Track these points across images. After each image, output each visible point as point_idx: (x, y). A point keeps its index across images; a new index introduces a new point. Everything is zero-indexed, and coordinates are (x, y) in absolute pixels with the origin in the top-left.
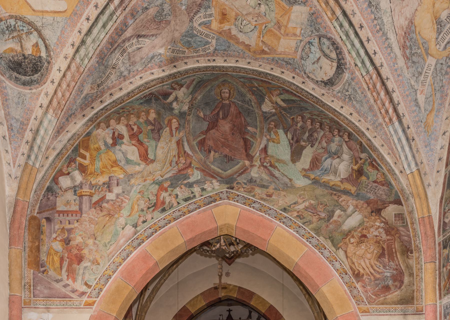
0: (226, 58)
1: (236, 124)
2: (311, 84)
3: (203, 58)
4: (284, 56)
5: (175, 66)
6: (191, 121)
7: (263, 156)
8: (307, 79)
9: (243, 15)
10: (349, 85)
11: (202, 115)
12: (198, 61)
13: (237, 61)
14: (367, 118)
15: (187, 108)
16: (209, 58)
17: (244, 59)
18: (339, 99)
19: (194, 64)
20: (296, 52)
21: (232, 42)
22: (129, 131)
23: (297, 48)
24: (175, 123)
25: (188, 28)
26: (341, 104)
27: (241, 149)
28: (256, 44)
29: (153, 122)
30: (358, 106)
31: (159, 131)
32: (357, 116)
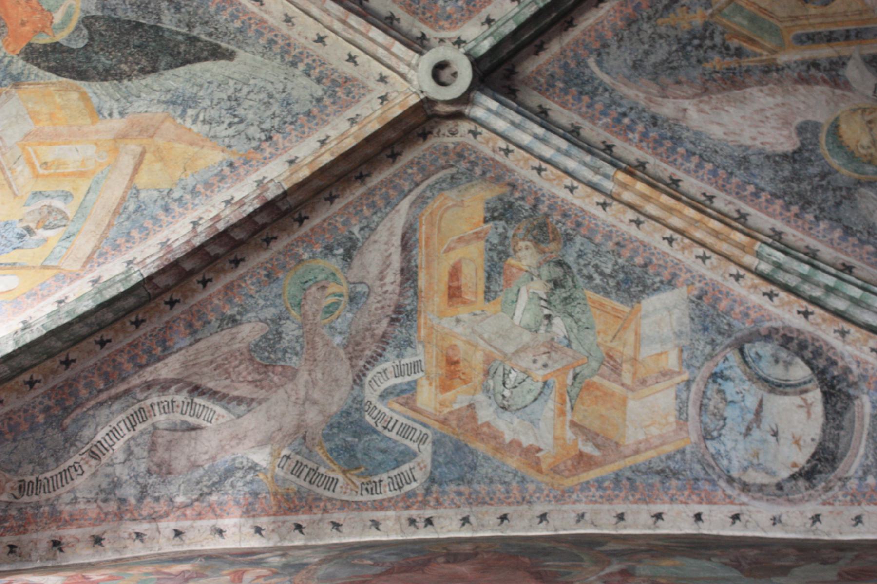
0: (465, 511)
3: (391, 513)
4: (651, 454)
5: (299, 527)
8: (744, 498)
9: (505, 355)
12: (376, 524)
13: (504, 518)
16: (414, 513)
17: (525, 507)
19: (361, 534)
21: (481, 447)
25: (349, 402)
28: (556, 438)
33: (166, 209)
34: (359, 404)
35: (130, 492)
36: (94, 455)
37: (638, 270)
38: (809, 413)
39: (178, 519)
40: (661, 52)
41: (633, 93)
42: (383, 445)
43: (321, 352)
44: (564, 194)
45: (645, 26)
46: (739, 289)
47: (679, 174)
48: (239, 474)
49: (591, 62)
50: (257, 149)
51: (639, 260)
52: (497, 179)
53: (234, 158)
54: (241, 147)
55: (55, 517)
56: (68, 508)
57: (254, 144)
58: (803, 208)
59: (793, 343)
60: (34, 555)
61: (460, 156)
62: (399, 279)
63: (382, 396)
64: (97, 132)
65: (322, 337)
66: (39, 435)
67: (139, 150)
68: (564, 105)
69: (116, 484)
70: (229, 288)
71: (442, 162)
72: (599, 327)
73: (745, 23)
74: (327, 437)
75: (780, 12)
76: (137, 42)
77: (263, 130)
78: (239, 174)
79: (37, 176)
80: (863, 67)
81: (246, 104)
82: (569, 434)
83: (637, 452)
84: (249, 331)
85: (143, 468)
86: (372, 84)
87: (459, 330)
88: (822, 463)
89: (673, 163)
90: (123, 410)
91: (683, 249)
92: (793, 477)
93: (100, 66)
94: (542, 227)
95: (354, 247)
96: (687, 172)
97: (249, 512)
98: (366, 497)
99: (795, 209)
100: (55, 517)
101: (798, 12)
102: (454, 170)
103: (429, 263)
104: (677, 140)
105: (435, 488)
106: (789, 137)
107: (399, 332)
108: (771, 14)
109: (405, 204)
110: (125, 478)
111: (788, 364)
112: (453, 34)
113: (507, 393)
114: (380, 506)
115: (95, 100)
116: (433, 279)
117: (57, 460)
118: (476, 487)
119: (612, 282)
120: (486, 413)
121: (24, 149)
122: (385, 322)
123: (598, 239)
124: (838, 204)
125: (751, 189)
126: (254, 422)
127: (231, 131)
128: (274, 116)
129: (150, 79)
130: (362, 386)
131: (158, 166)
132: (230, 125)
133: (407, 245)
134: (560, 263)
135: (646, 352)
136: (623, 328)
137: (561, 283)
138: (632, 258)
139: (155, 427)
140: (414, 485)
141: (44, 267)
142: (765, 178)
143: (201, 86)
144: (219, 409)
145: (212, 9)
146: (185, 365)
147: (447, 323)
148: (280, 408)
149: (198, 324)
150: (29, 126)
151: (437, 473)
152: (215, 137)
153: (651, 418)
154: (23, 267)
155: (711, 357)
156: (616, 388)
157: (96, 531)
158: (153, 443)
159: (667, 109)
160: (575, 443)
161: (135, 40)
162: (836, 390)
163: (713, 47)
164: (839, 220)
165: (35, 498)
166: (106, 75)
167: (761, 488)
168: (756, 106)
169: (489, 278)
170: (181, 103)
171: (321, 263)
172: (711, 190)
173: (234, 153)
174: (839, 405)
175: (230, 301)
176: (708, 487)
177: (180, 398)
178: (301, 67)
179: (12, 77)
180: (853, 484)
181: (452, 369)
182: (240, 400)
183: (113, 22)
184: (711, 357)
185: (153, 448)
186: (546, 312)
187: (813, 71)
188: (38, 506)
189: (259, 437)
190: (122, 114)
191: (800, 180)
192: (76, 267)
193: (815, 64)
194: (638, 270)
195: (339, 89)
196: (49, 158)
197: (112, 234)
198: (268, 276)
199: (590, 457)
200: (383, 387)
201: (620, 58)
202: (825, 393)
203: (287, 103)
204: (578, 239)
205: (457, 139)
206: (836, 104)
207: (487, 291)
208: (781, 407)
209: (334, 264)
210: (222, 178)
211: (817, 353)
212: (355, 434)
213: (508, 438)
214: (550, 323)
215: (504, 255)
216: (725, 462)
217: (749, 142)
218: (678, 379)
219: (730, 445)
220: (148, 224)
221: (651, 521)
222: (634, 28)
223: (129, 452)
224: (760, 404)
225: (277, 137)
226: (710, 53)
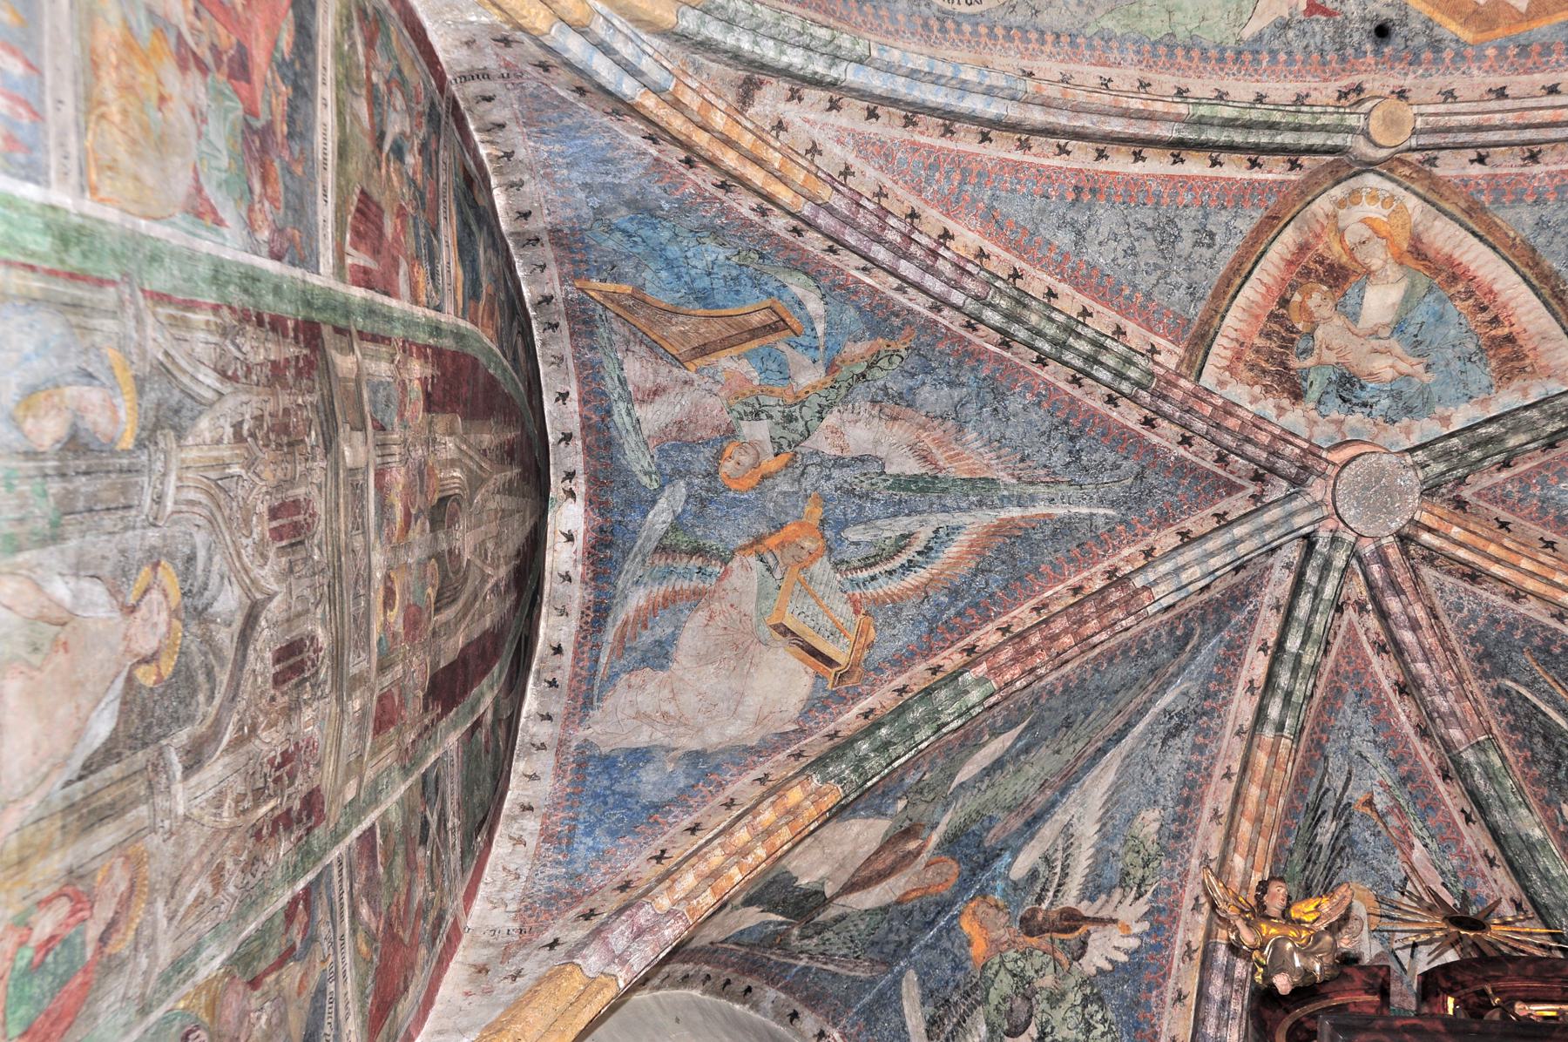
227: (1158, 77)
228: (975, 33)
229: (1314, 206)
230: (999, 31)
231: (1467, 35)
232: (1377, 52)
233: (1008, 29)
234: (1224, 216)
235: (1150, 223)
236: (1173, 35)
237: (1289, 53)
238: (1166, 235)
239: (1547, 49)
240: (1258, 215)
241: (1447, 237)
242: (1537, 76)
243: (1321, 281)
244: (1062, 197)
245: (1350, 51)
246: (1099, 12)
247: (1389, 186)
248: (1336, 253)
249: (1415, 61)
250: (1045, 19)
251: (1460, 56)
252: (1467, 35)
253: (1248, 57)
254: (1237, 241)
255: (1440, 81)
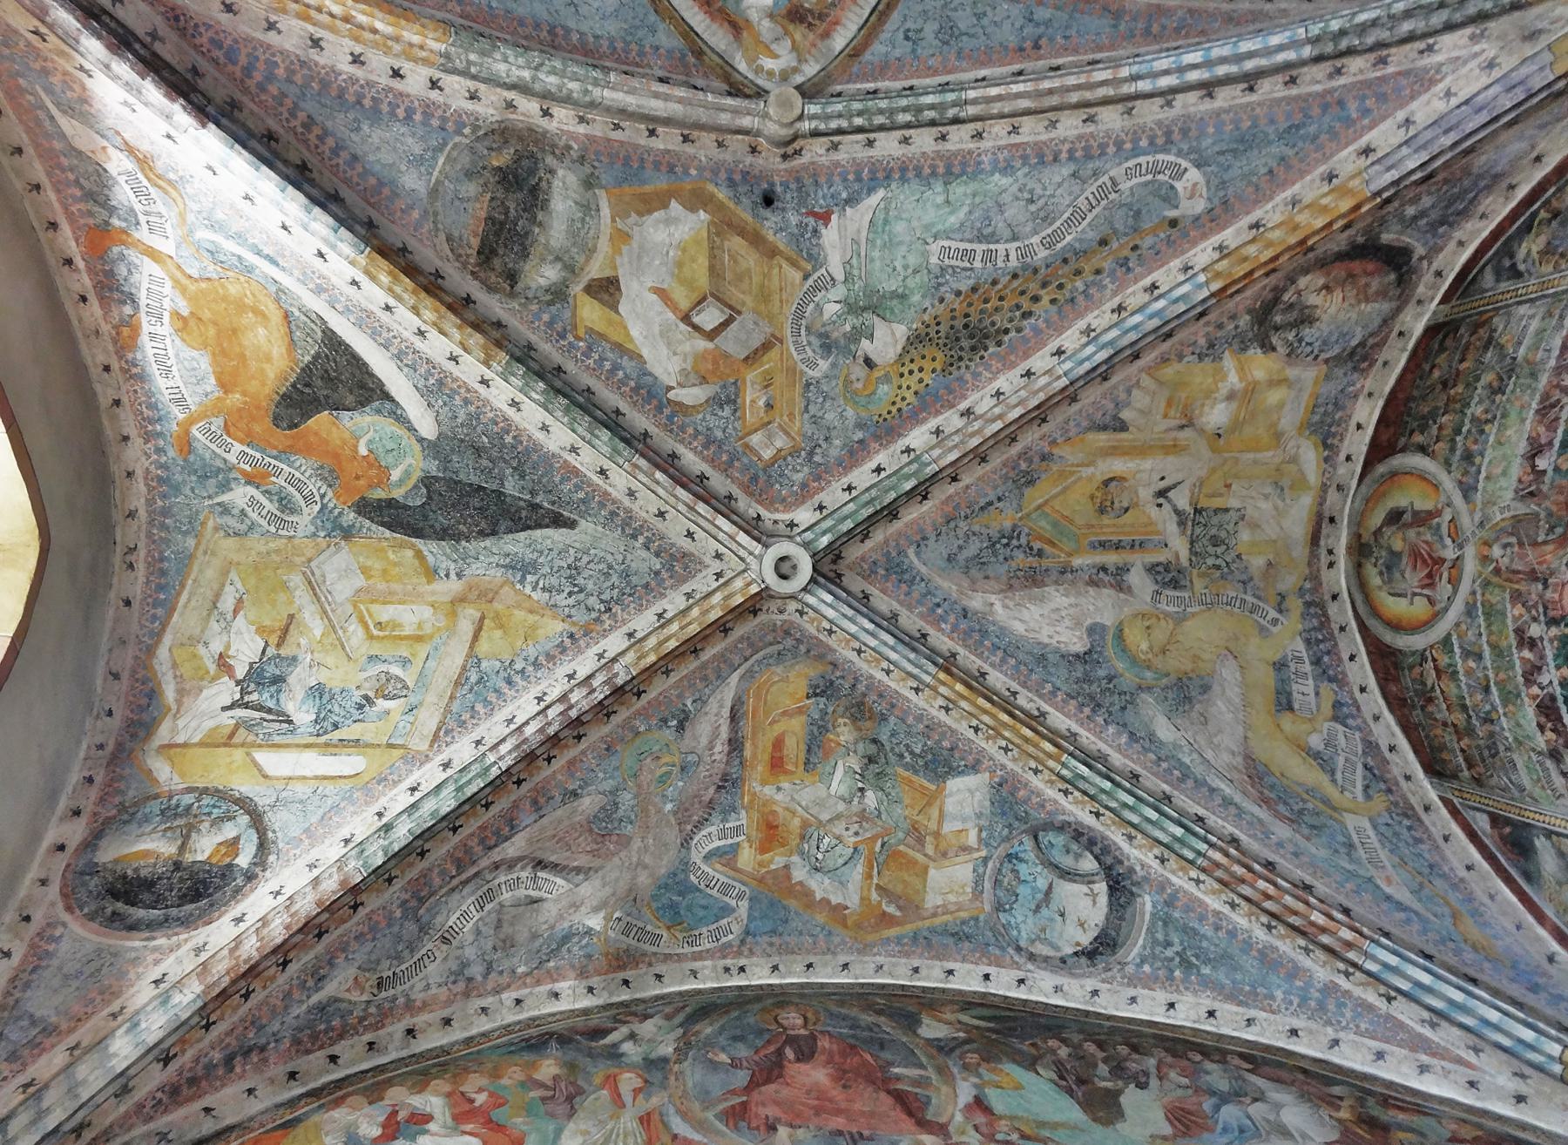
0: (776, 960)
1: (846, 1067)
2: (1045, 974)
3: (708, 963)
5: (626, 982)
6: (688, 1073)
7: (981, 1119)
8: (1030, 966)
10: (1165, 924)
11: (723, 1058)
12: (694, 973)
13: (809, 966)
14: (1273, 998)
15: (671, 1050)
16: (728, 962)
17: (829, 957)
18: (1149, 982)
19: (681, 983)
20: (978, 892)
22: (453, 1106)
23: (979, 881)
24: (628, 1081)
26: (1162, 996)
27: (893, 1113)
29: (550, 1083)
30: (1221, 976)
31: (570, 1099)
32: (1235, 1008)
33: (509, 682)
34: (686, 866)
35: (476, 970)
36: (445, 940)
37: (945, 753)
38: (1094, 902)
39: (518, 988)
40: (973, 549)
41: (947, 585)
42: (703, 902)
43: (654, 819)
44: (880, 675)
45: (962, 524)
46: (1037, 782)
47: (986, 668)
48: (576, 940)
49: (911, 552)
50: (597, 620)
51: (946, 744)
52: (820, 657)
53: (574, 630)
54: (581, 617)
55: (410, 1007)
56: (421, 995)
57: (594, 615)
58: (1093, 710)
59: (1082, 837)
60: (390, 1047)
61: (787, 633)
62: (726, 748)
63: (706, 858)
64: (433, 593)
65: (655, 805)
66: (396, 929)
67: (478, 615)
68: (884, 591)
69: (465, 965)
70: (571, 763)
71: (770, 638)
72: (907, 801)
73: (1049, 527)
74: (654, 897)
75: (1080, 521)
76: (477, 505)
77: (602, 601)
78: (579, 647)
79: (371, 637)
80: (1143, 572)
81: (586, 573)
82: (874, 896)
83: (935, 915)
84: (588, 804)
85: (490, 945)
86: (707, 560)
87: (779, 797)
88: (1102, 948)
89: (980, 656)
90: (473, 893)
91: (987, 739)
92: (1076, 954)
93: (438, 526)
94: (861, 704)
95: (686, 718)
96: (992, 665)
97: (582, 974)
98: (687, 949)
99: (1087, 710)
100: (410, 1007)
101: (1094, 522)
102: (781, 647)
103: (754, 734)
104: (984, 633)
105: (749, 939)
106: (1081, 638)
107: (724, 798)
108: (1071, 522)
109: (735, 677)
110: (473, 957)
111: (1078, 856)
112: (786, 517)
113: (820, 856)
114: (698, 957)
115: (430, 559)
116: (757, 750)
117: (412, 951)
118: (787, 939)
119: (921, 762)
120: (799, 874)
121: (355, 606)
122: (712, 790)
123: (910, 720)
124: (1123, 709)
125: (1049, 687)
126: (589, 890)
127: (571, 601)
128: (613, 587)
129: (488, 542)
130: (689, 849)
131: (498, 633)
132: (570, 594)
133: (734, 717)
134: (875, 741)
135: (947, 828)
136: (929, 804)
137: (874, 762)
138: (939, 741)
139: (501, 905)
140: (731, 937)
141: (391, 746)
142: (1060, 677)
143: (541, 552)
144: (559, 881)
145: (557, 479)
146: (530, 842)
147: (769, 791)
148: (614, 875)
149: (542, 800)
150: (360, 581)
151: (752, 926)
152: (555, 606)
153: (949, 884)
154: (368, 745)
155: (1007, 839)
156: (919, 857)
157: (445, 1013)
158: (499, 920)
159: (976, 602)
160: (880, 903)
161: (476, 502)
162: (1120, 886)
163: (1019, 547)
164: (1125, 725)
165: (392, 992)
166: (443, 534)
167: (1046, 959)
168: (1053, 605)
169: (809, 751)
170: (522, 568)
171: (657, 735)
172: (1015, 686)
173: (574, 624)
174: (1122, 900)
175: (572, 776)
176: (997, 952)
177: (524, 874)
178: (641, 539)
179: (341, 528)
180: (1130, 969)
181: (771, 833)
182: (578, 870)
183: (453, 484)
184: (1007, 839)
185: (499, 925)
186: (860, 785)
187: (1102, 574)
188: (395, 998)
189: (595, 903)
190: (459, 575)
191: (1091, 682)
192: (424, 747)
193: (1104, 569)
194: (945, 753)
195: (678, 564)
196: (384, 618)
197: (455, 707)
198: (607, 750)
199: (892, 916)
200: (707, 849)
201: (937, 550)
202: (1110, 887)
203: (625, 575)
204: (892, 719)
205: (784, 617)
206: (1121, 608)
207: (807, 762)
208: (1071, 894)
209: (668, 734)
210: (563, 651)
211: (1106, 850)
212: (680, 894)
213: (818, 897)
214: (863, 796)
215: (824, 729)
216: (1015, 933)
217: (1046, 640)
218: (976, 855)
219: (1020, 919)
220: (492, 697)
221: (943, 976)
222: (952, 524)
223: (478, 932)
224: (1050, 886)
225: (616, 609)
226: (1016, 553)
227: (964, 146)
228: (1135, 141)
229: (818, 67)
230: (1111, 150)
231: (711, 187)
232: (772, 184)
233: (1103, 154)
234: (897, 53)
235: (964, 38)
236: (945, 184)
237: (845, 180)
238: (949, 33)
239: (657, 165)
240: (867, 56)
241: (715, 36)
242: (662, 147)
243: (809, 11)
244: (1051, 39)
245: (793, 186)
246: (1014, 188)
247: (760, 82)
248: (799, 32)
249: (745, 174)
250: (1072, 167)
251: (715, 172)
252: (711, 187)
253: (880, 175)
254: (884, 36)
255: (727, 156)
